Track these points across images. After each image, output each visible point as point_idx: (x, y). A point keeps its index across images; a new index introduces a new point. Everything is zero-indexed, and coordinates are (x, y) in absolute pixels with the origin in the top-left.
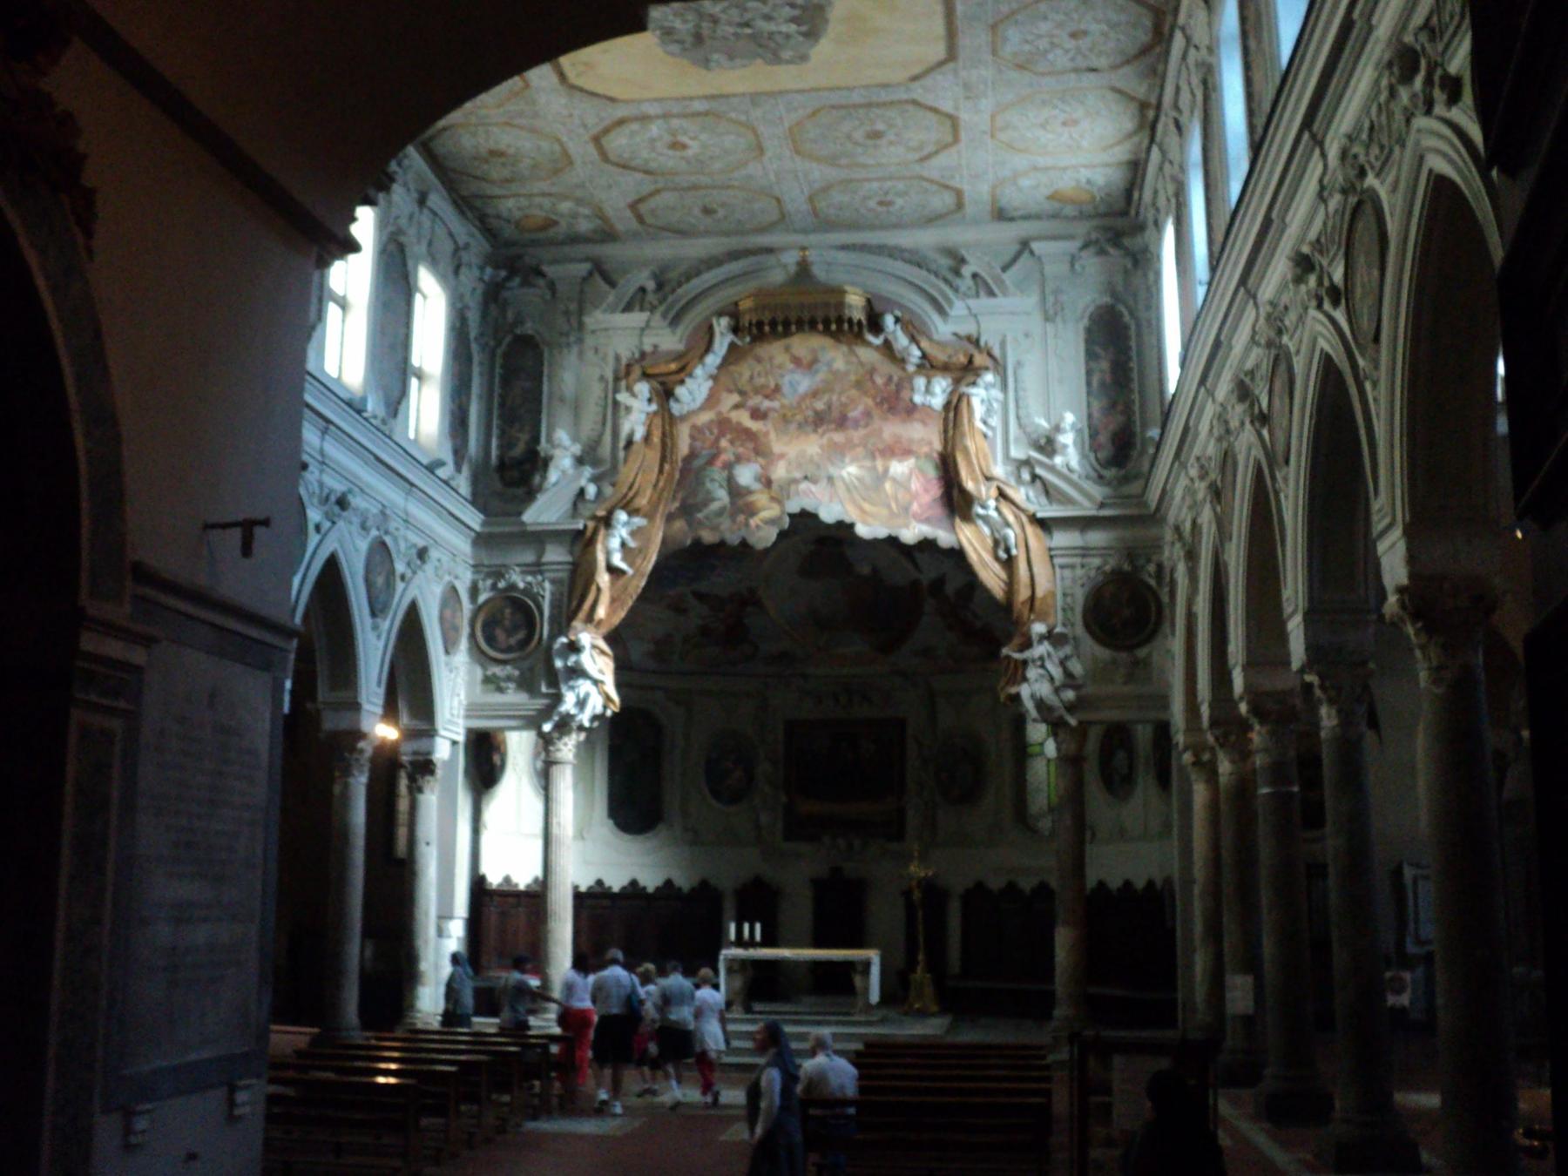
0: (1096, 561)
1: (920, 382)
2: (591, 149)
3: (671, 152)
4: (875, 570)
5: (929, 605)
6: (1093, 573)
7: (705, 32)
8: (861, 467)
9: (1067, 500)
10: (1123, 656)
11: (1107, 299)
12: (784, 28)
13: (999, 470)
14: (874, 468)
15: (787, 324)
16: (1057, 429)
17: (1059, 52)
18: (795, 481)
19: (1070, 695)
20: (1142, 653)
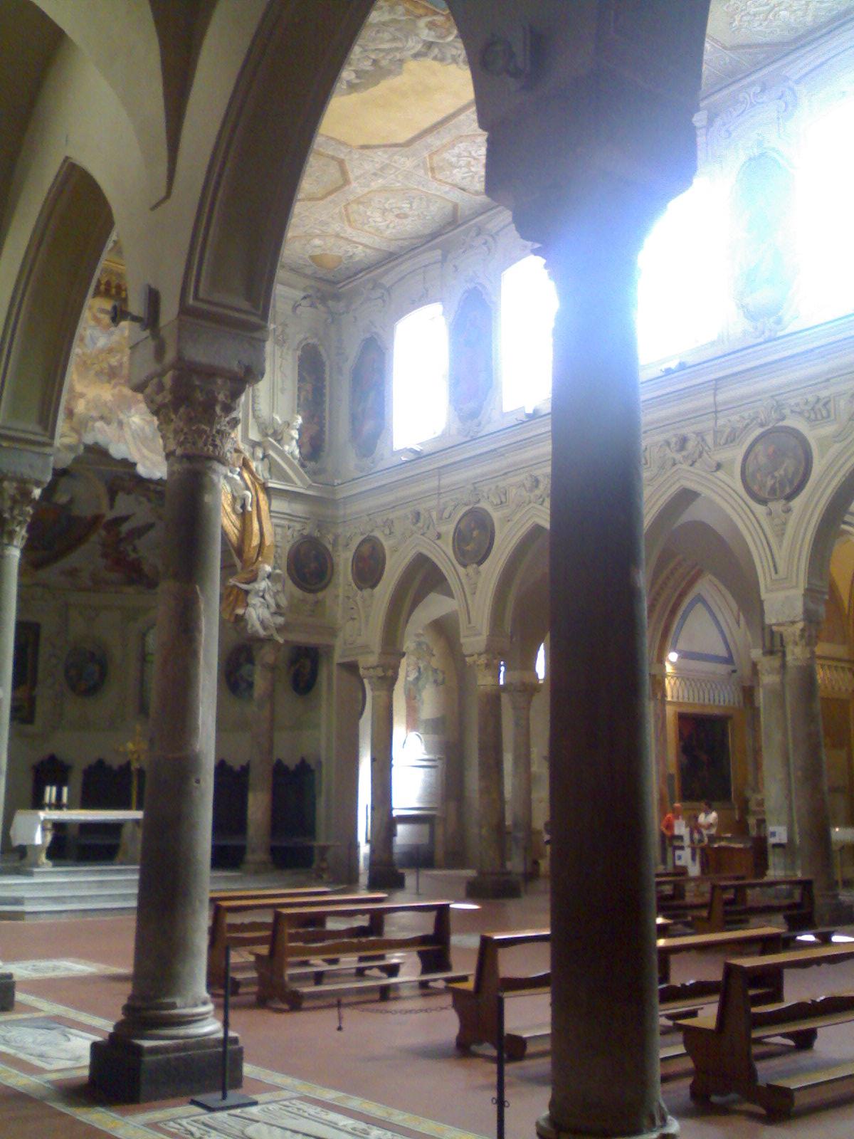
0: (298, 526)
4: (71, 501)
5: (97, 537)
6: (295, 534)
8: (144, 419)
9: (284, 477)
10: (310, 597)
11: (313, 341)
13: (242, 446)
16: (288, 425)
17: (465, 170)
19: (280, 620)
20: (320, 595)
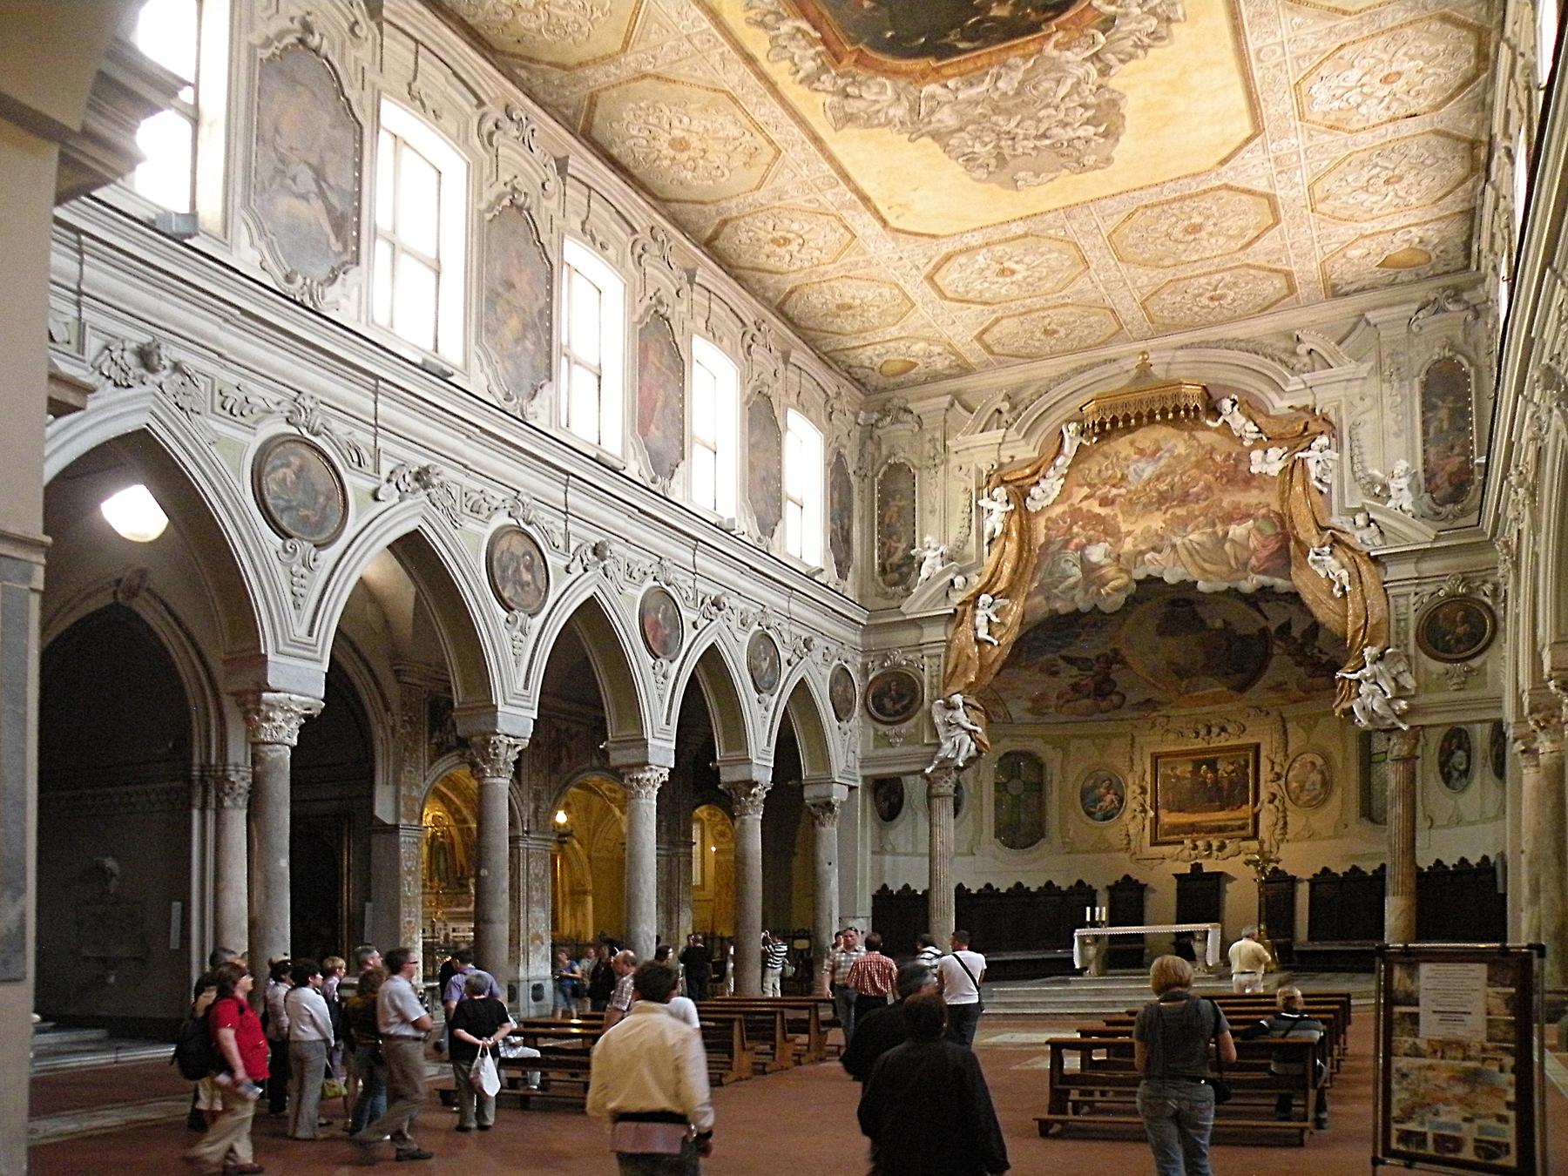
1: (1256, 455)
2: (927, 287)
3: (1001, 280)
5: (1278, 649)
7: (1007, 152)
12: (1081, 133)
14: (1215, 533)
15: (1127, 419)
18: (1142, 553)
